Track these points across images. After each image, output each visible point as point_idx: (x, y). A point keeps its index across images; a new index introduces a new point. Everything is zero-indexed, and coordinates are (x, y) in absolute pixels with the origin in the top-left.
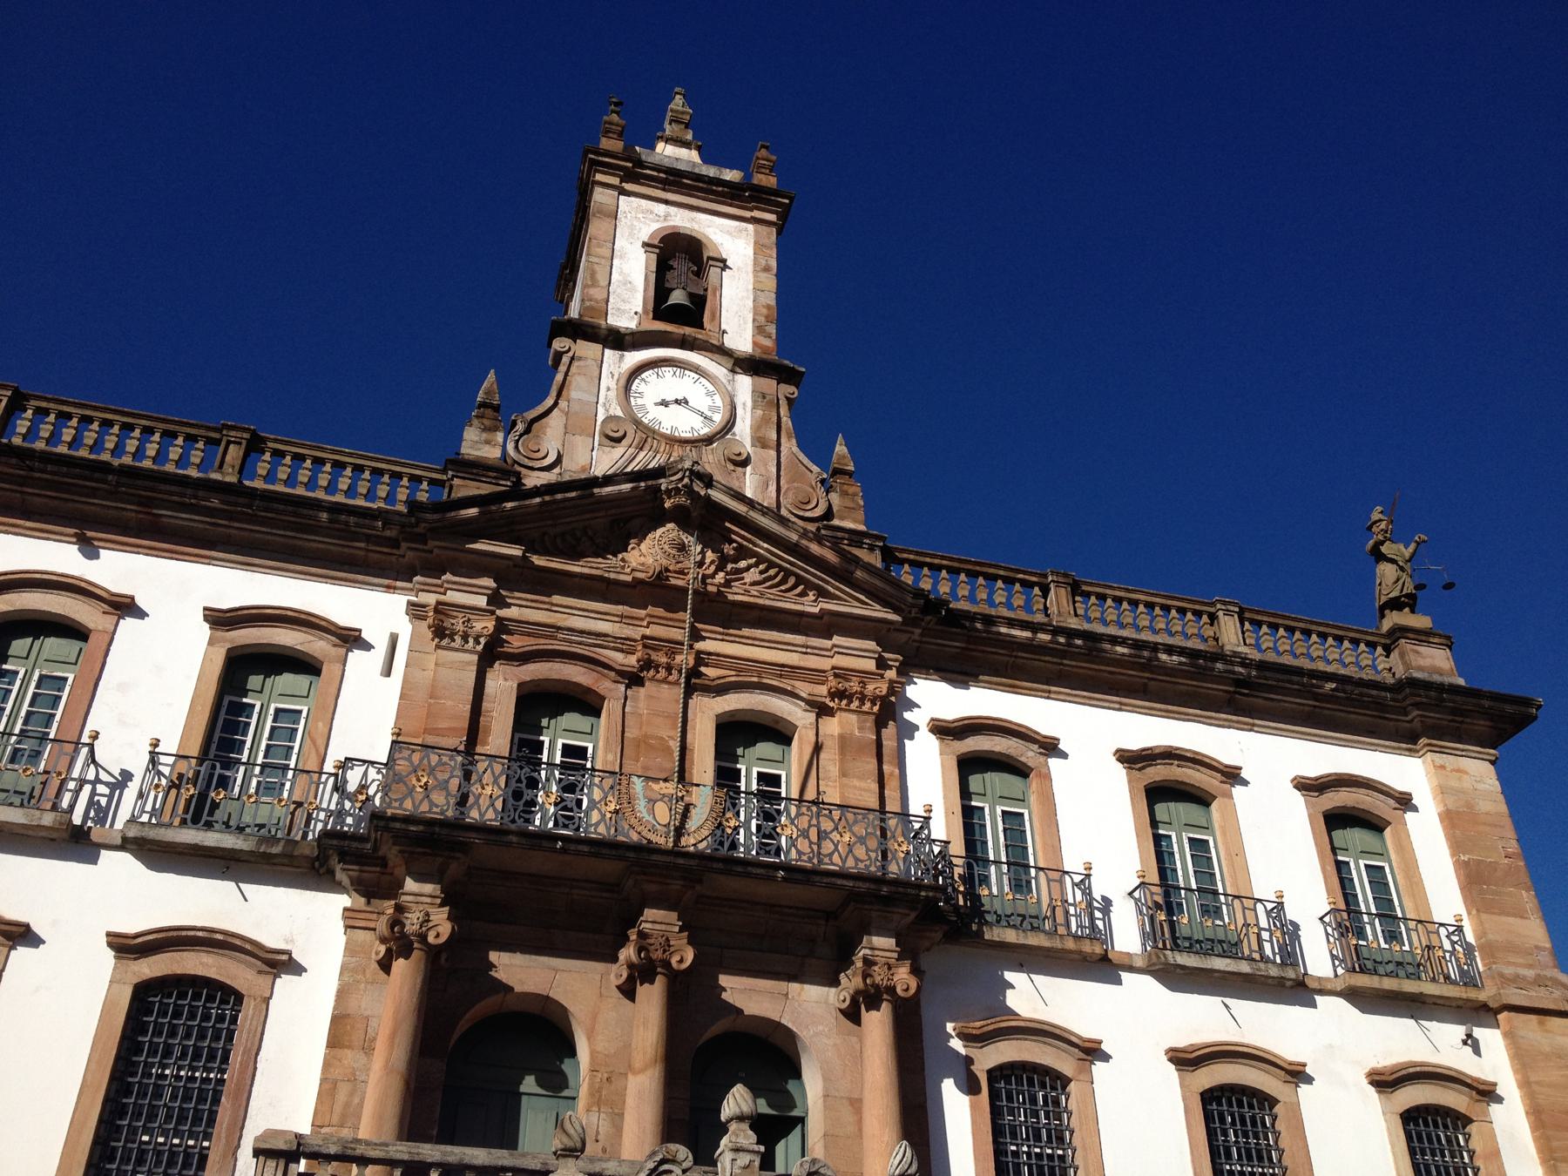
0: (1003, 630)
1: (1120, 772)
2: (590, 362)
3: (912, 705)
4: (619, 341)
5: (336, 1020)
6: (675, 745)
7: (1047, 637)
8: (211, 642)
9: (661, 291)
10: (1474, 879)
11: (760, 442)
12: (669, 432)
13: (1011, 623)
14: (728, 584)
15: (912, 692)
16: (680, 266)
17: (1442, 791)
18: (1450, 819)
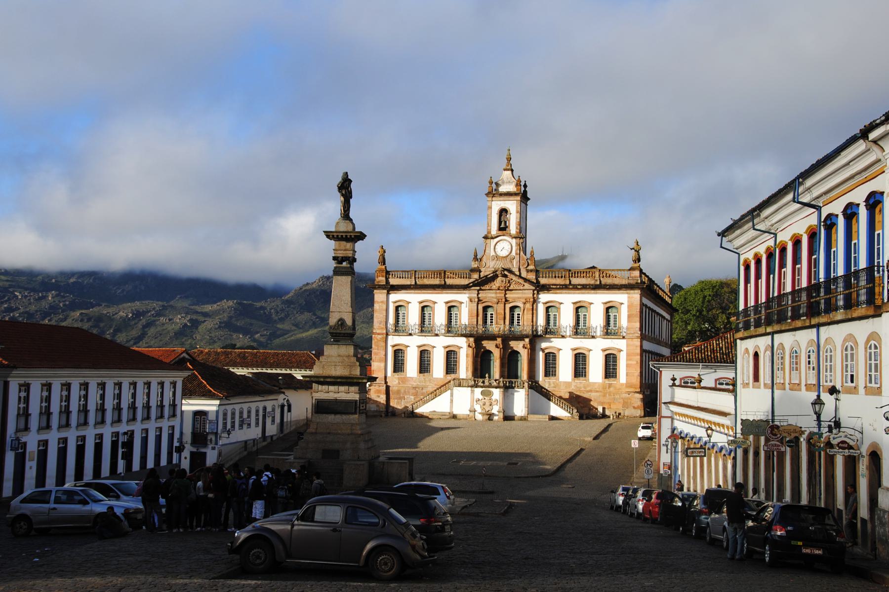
0: (552, 287)
1: (572, 305)
2: (489, 244)
3: (539, 299)
4: (493, 238)
5: (467, 354)
6: (503, 313)
7: (558, 287)
8: (446, 306)
9: (500, 223)
10: (629, 316)
11: (516, 254)
12: (501, 256)
13: (553, 285)
14: (509, 286)
15: (540, 296)
16: (504, 214)
17: (628, 301)
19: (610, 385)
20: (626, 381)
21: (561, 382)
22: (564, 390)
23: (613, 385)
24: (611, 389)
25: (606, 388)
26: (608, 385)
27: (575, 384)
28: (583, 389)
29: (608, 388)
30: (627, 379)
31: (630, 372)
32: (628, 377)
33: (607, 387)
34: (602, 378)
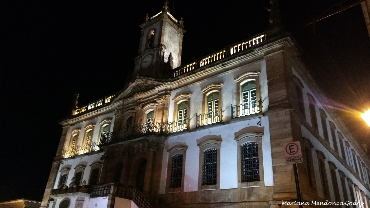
18: (267, 72)
19: (250, 192)
20: (274, 182)
21: (186, 193)
22: (188, 204)
23: (255, 191)
24: (253, 199)
25: (244, 198)
26: (246, 192)
27: (203, 195)
28: (212, 201)
29: (247, 197)
30: (274, 178)
31: (278, 165)
32: (274, 175)
33: (246, 197)
34: (238, 182)
